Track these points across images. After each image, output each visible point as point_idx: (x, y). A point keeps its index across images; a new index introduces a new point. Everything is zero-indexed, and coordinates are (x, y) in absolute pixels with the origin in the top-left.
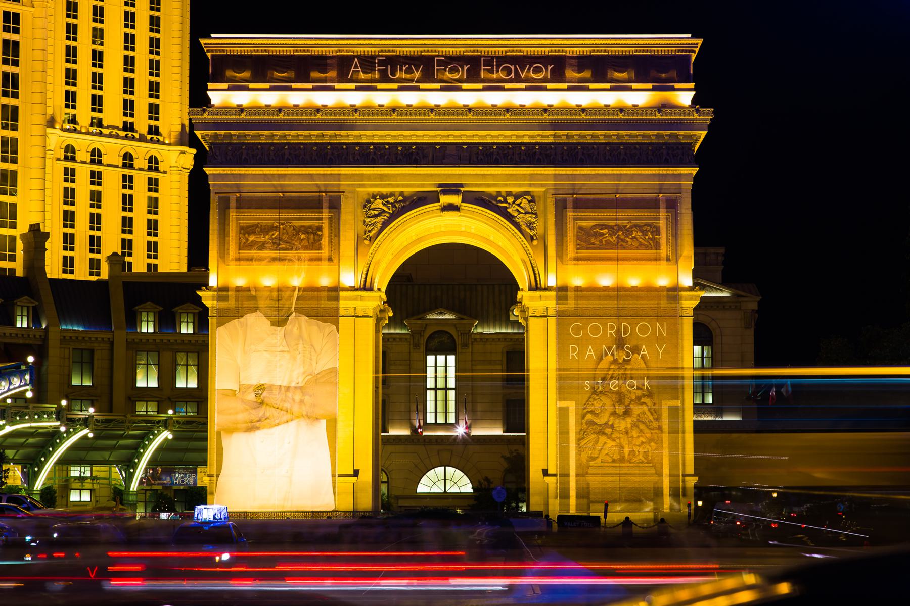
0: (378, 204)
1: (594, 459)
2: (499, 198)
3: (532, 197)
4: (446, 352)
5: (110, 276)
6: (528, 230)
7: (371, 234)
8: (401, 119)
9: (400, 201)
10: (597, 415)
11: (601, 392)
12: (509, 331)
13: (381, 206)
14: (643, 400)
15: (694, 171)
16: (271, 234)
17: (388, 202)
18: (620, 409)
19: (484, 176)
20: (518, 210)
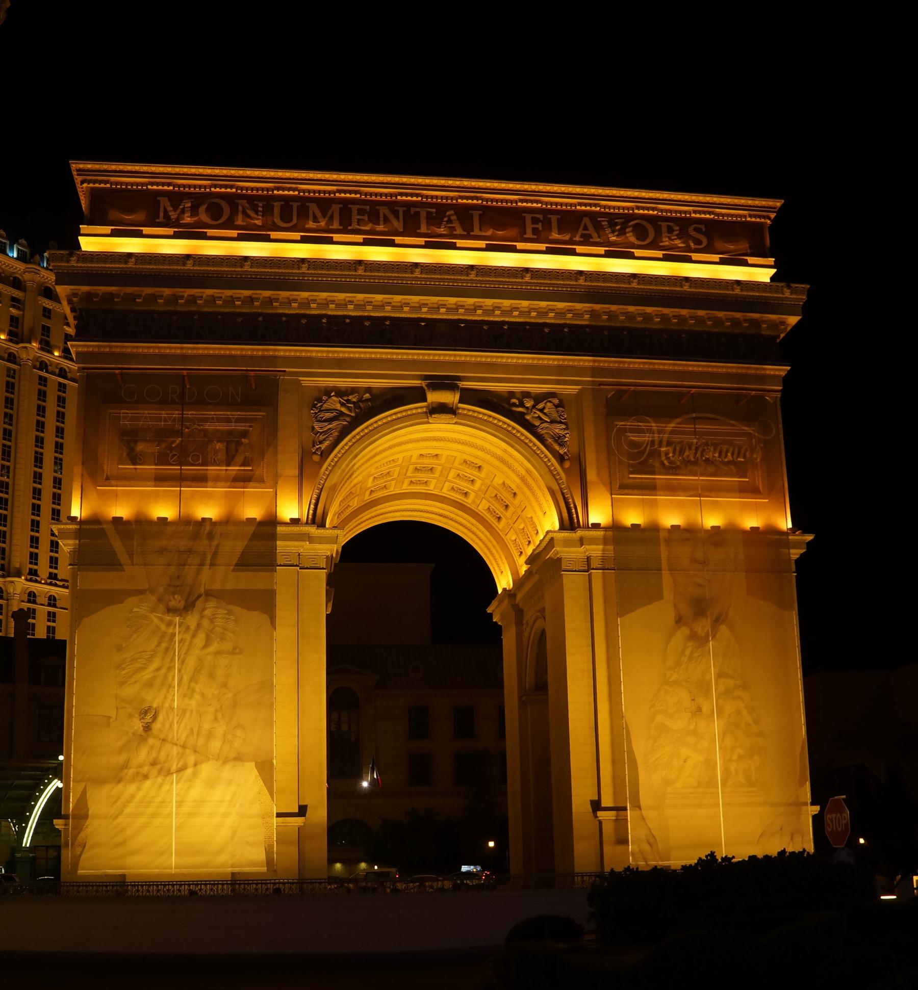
0: (334, 403)
3: (560, 400)
6: (557, 447)
7: (323, 446)
8: (370, 277)
9: (367, 400)
13: (338, 406)
17: (348, 401)
19: (490, 367)
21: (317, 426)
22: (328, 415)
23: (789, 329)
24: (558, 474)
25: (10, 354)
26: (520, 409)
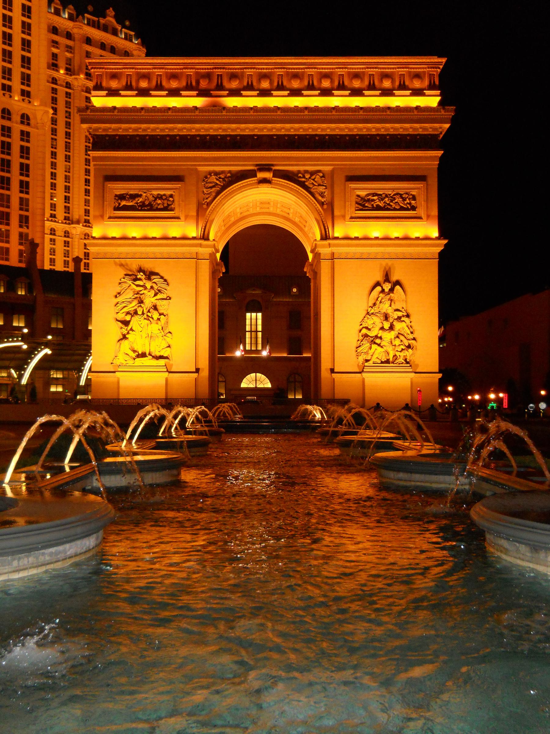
0: (213, 179)
1: (367, 361)
2: (300, 175)
4: (257, 311)
5: (75, 270)
6: (320, 198)
9: (229, 177)
10: (369, 330)
11: (372, 314)
12: (291, 300)
13: (215, 180)
14: (403, 319)
15: (440, 153)
16: (137, 199)
17: (220, 178)
18: (387, 325)
20: (313, 184)
21: (205, 190)
22: (210, 185)
23: (445, 131)
24: (320, 212)
25: (67, 83)
26: (303, 179)
